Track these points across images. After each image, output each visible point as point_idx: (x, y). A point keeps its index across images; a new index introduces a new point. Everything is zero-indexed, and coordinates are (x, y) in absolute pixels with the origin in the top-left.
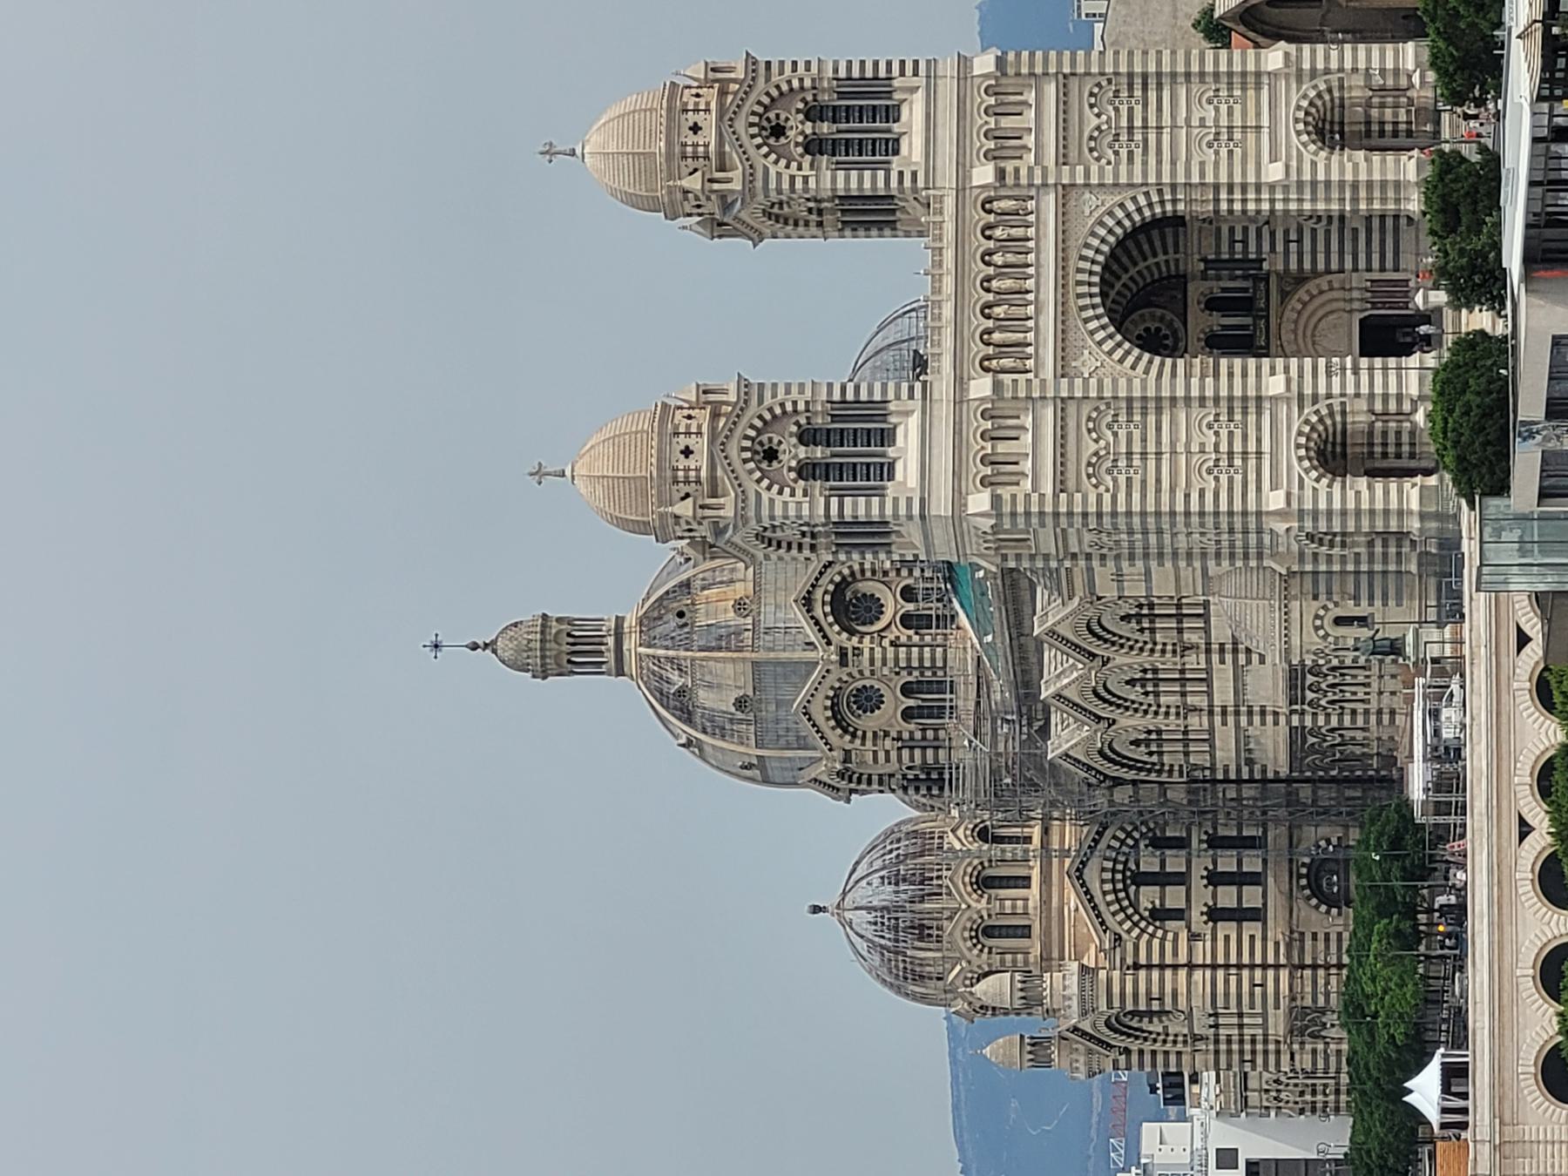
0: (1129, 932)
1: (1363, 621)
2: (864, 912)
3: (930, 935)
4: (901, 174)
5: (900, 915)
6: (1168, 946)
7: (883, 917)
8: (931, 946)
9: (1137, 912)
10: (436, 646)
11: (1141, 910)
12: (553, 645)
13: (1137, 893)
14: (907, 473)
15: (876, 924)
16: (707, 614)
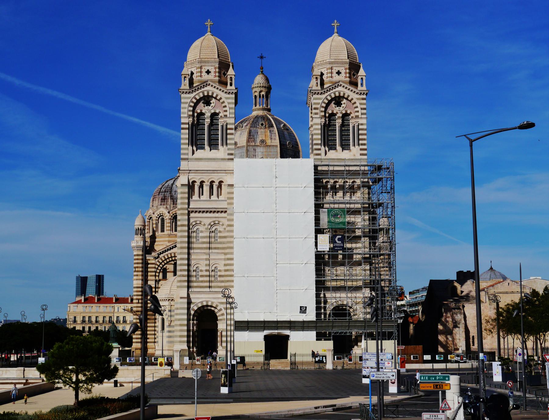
0: (158, 261)
1: (163, 328)
2: (172, 183)
3: (162, 202)
4: (320, 149)
5: (169, 193)
6: (154, 274)
7: (169, 188)
8: (160, 202)
9: (165, 264)
10: (262, 57)
11: (166, 265)
12: (259, 90)
13: (172, 264)
14: (200, 153)
15: (168, 186)
16: (262, 132)
